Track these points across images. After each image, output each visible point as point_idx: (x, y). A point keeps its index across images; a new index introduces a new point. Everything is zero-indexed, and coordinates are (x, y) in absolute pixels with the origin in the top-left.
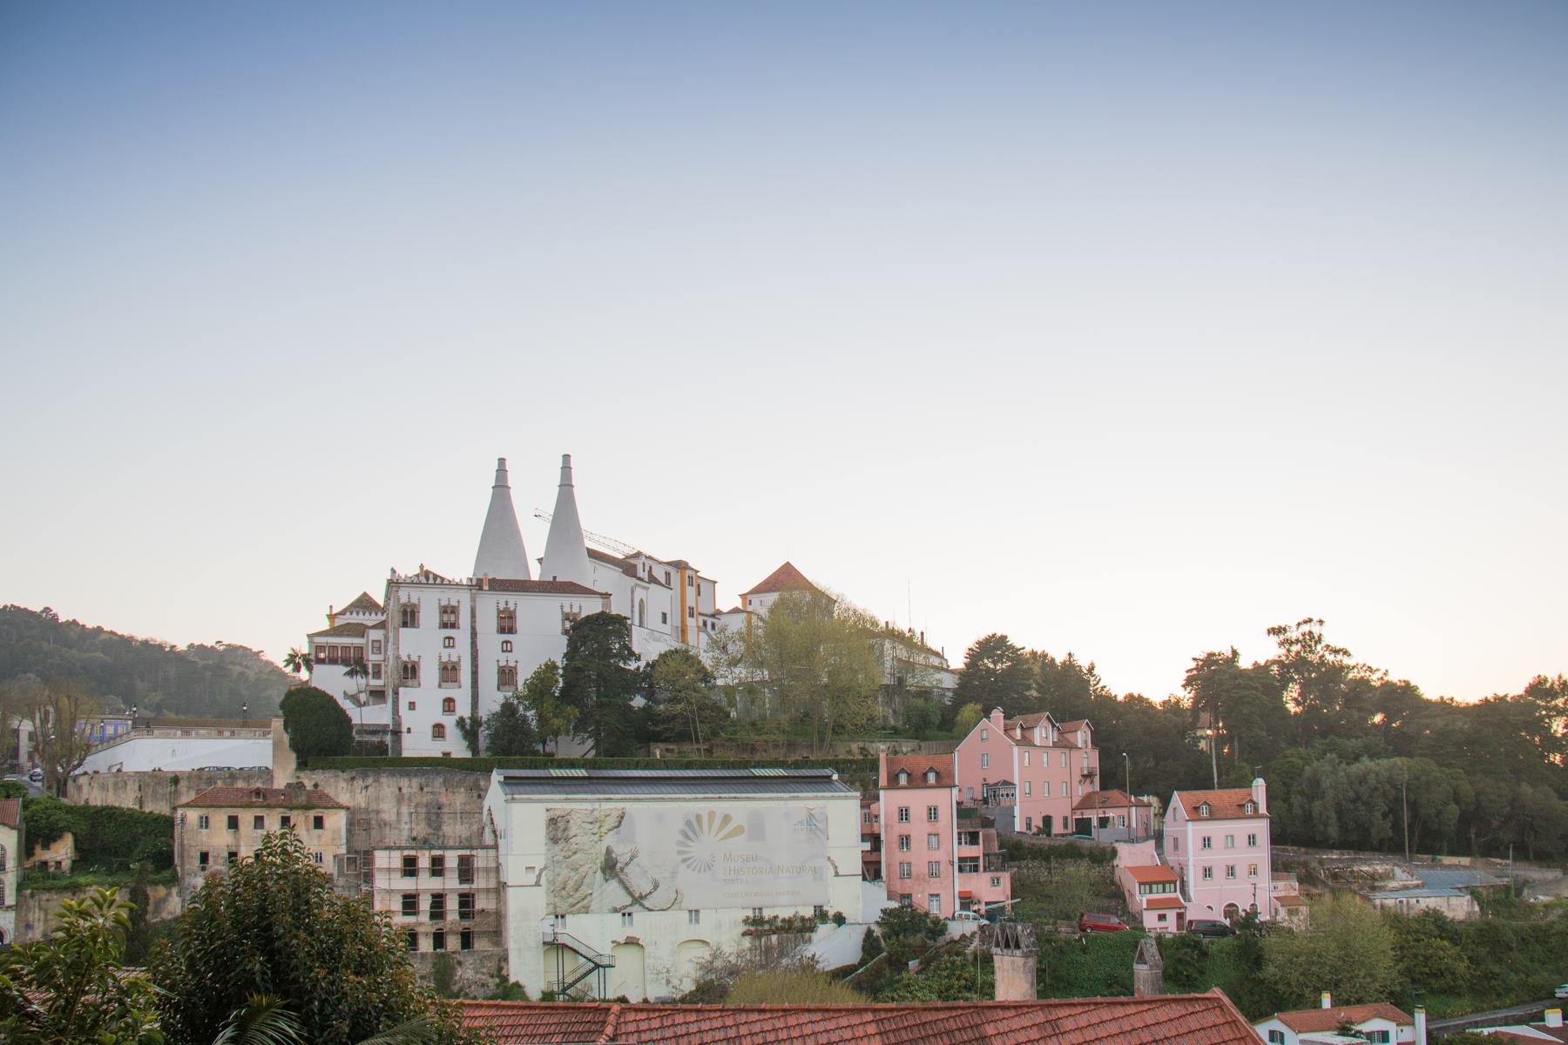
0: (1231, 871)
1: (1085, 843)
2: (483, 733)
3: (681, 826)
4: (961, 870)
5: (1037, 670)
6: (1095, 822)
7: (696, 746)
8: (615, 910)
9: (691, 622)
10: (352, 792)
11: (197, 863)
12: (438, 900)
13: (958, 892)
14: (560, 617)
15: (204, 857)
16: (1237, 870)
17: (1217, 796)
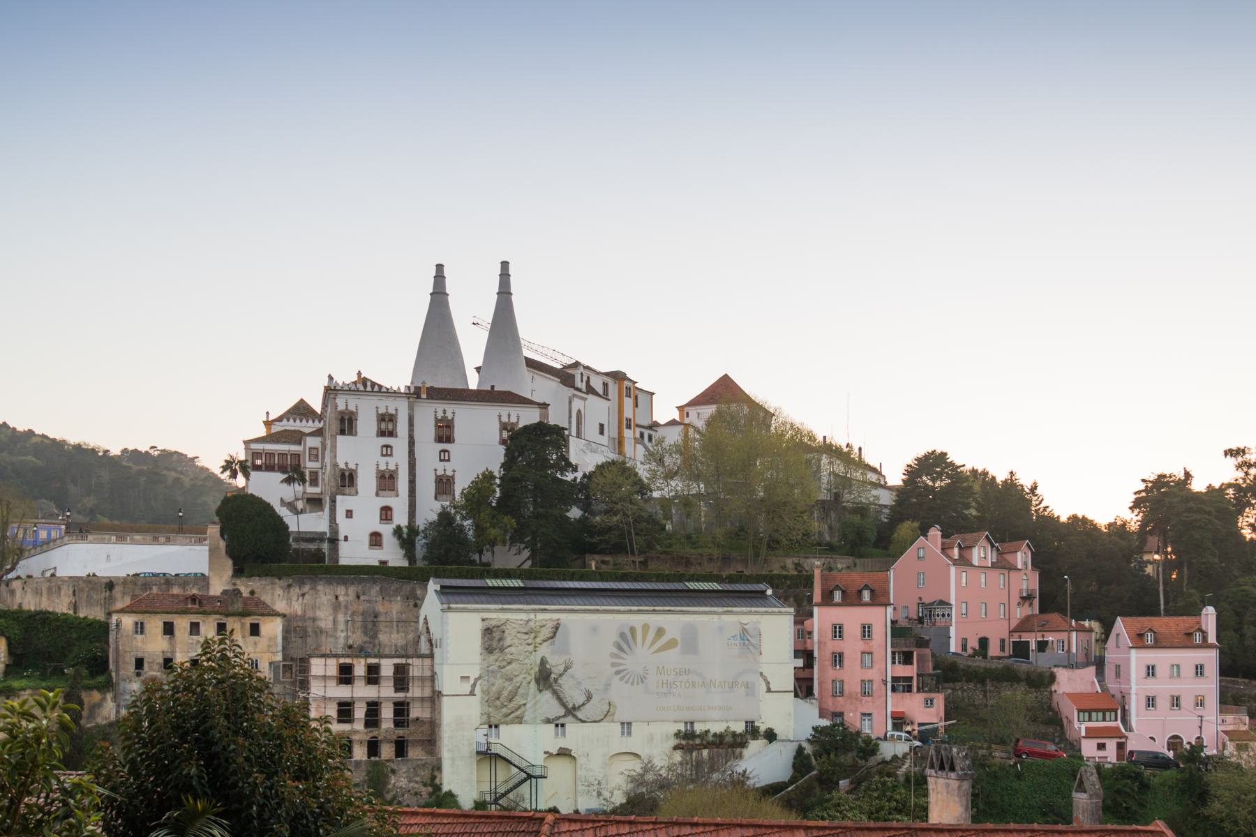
0: (1176, 702)
1: (1022, 667)
2: (420, 542)
3: (615, 637)
4: (894, 689)
5: (977, 487)
6: (1033, 646)
7: (631, 558)
8: (548, 721)
9: (628, 433)
10: (289, 600)
11: (132, 668)
12: (373, 709)
13: (892, 712)
14: (498, 426)
15: (139, 663)
16: (1183, 703)
17: (1162, 623)
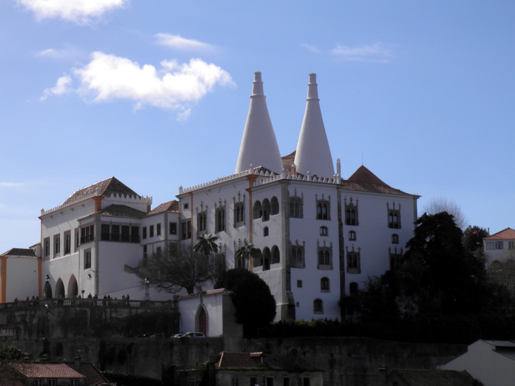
14: (386, 213)
